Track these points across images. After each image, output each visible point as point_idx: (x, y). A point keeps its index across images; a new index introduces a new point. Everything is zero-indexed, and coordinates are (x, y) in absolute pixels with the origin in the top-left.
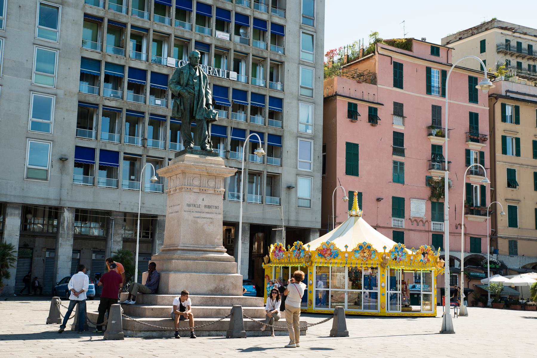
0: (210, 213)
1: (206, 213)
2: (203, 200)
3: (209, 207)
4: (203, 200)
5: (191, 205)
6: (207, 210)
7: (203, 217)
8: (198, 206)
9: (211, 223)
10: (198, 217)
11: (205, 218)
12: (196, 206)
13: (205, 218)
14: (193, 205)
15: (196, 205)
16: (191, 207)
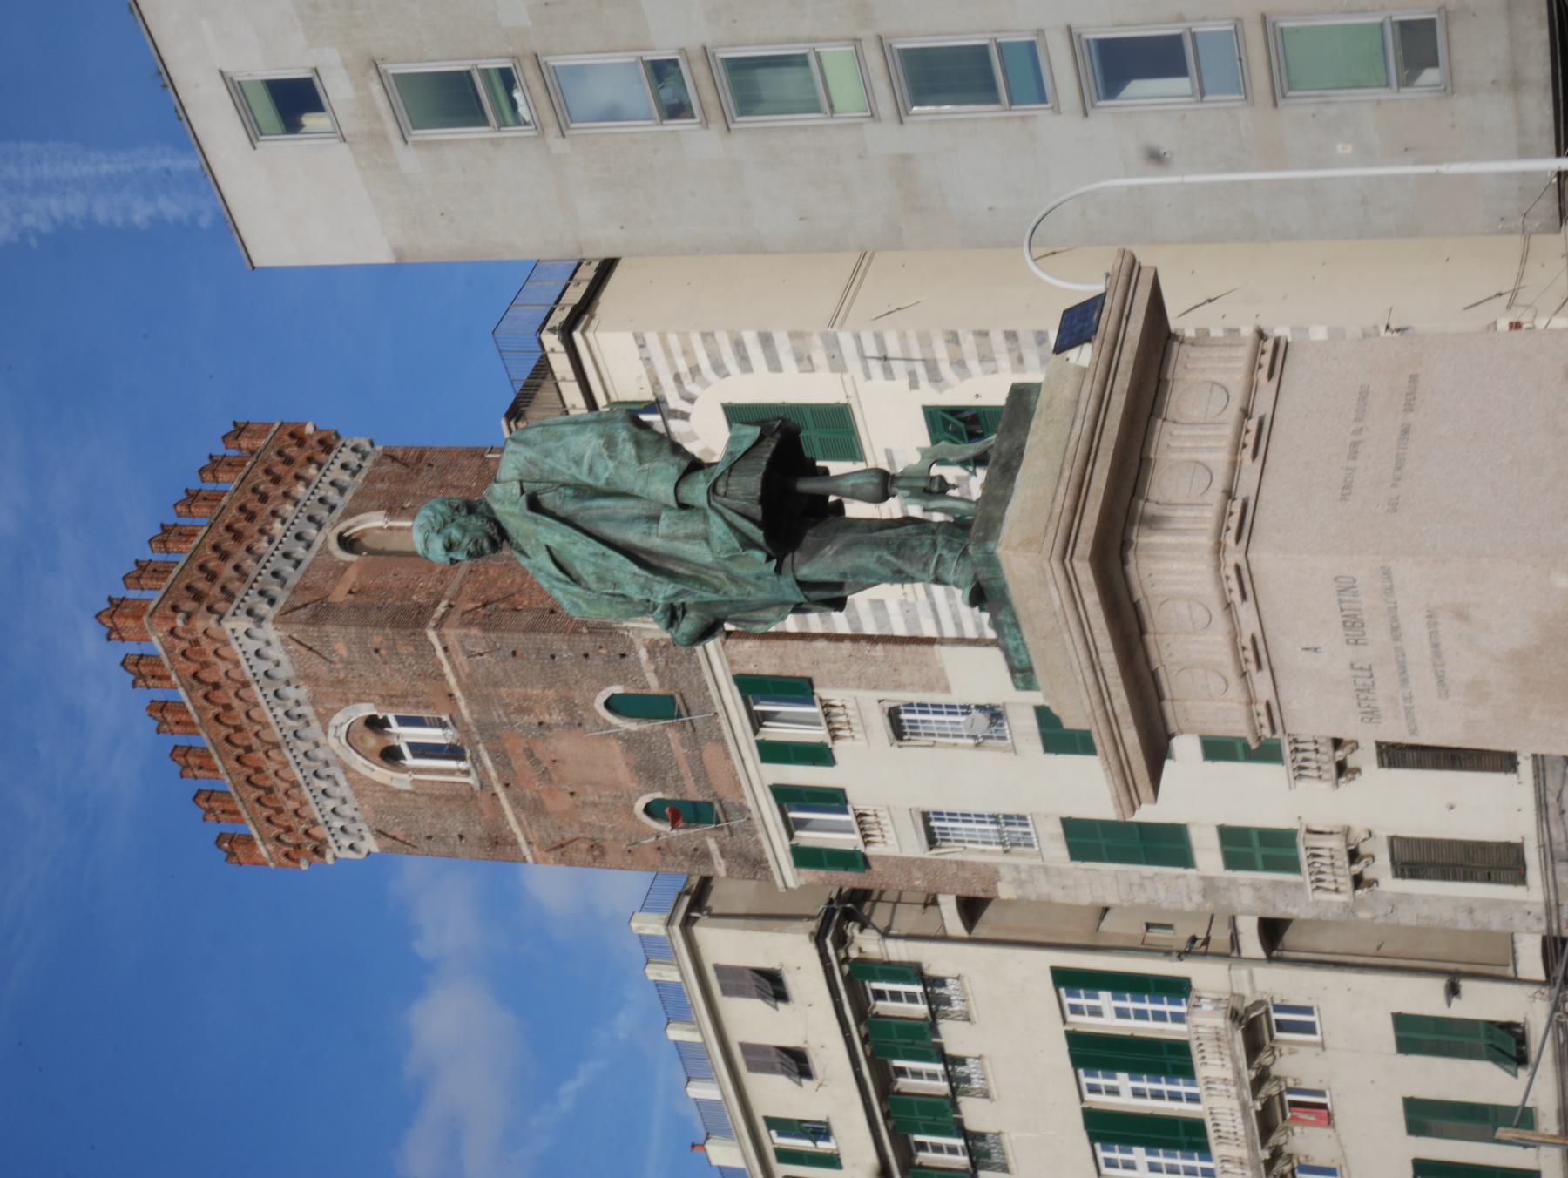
0: (1395, 618)
1: (1396, 639)
2: (1315, 650)
3: (1353, 624)
4: (1315, 650)
5: (1364, 704)
6: (1378, 635)
7: (1428, 652)
8: (1360, 673)
9: (1462, 615)
10: (1441, 680)
11: (1436, 645)
12: (1369, 681)
13: (1436, 645)
14: (1362, 696)
15: (1360, 682)
16: (1381, 704)
